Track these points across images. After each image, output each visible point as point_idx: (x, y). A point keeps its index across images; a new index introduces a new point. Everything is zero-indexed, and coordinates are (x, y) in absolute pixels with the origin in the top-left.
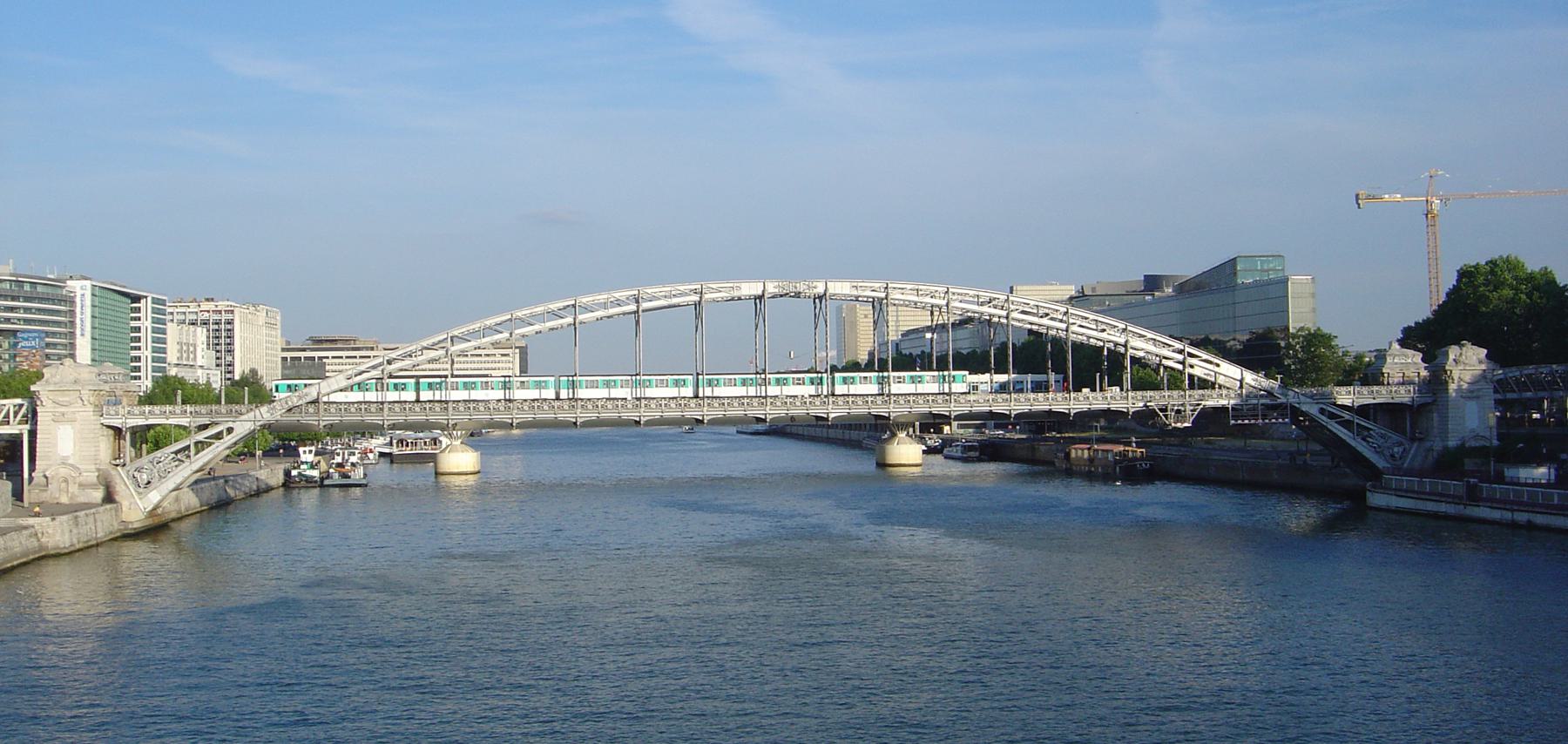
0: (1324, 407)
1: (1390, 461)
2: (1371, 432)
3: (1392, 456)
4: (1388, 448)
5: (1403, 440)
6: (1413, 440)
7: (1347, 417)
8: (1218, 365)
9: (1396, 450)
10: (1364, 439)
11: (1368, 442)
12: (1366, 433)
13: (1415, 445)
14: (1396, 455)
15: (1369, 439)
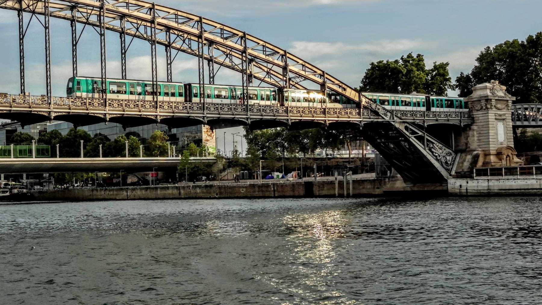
0: (408, 125)
1: (445, 166)
2: (434, 145)
3: (446, 163)
4: (444, 157)
5: (451, 151)
6: (456, 152)
7: (420, 133)
8: (345, 89)
9: (448, 158)
10: (430, 150)
11: (432, 152)
12: (432, 146)
13: (459, 155)
14: (449, 163)
15: (433, 150)
